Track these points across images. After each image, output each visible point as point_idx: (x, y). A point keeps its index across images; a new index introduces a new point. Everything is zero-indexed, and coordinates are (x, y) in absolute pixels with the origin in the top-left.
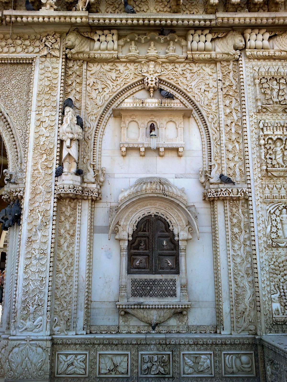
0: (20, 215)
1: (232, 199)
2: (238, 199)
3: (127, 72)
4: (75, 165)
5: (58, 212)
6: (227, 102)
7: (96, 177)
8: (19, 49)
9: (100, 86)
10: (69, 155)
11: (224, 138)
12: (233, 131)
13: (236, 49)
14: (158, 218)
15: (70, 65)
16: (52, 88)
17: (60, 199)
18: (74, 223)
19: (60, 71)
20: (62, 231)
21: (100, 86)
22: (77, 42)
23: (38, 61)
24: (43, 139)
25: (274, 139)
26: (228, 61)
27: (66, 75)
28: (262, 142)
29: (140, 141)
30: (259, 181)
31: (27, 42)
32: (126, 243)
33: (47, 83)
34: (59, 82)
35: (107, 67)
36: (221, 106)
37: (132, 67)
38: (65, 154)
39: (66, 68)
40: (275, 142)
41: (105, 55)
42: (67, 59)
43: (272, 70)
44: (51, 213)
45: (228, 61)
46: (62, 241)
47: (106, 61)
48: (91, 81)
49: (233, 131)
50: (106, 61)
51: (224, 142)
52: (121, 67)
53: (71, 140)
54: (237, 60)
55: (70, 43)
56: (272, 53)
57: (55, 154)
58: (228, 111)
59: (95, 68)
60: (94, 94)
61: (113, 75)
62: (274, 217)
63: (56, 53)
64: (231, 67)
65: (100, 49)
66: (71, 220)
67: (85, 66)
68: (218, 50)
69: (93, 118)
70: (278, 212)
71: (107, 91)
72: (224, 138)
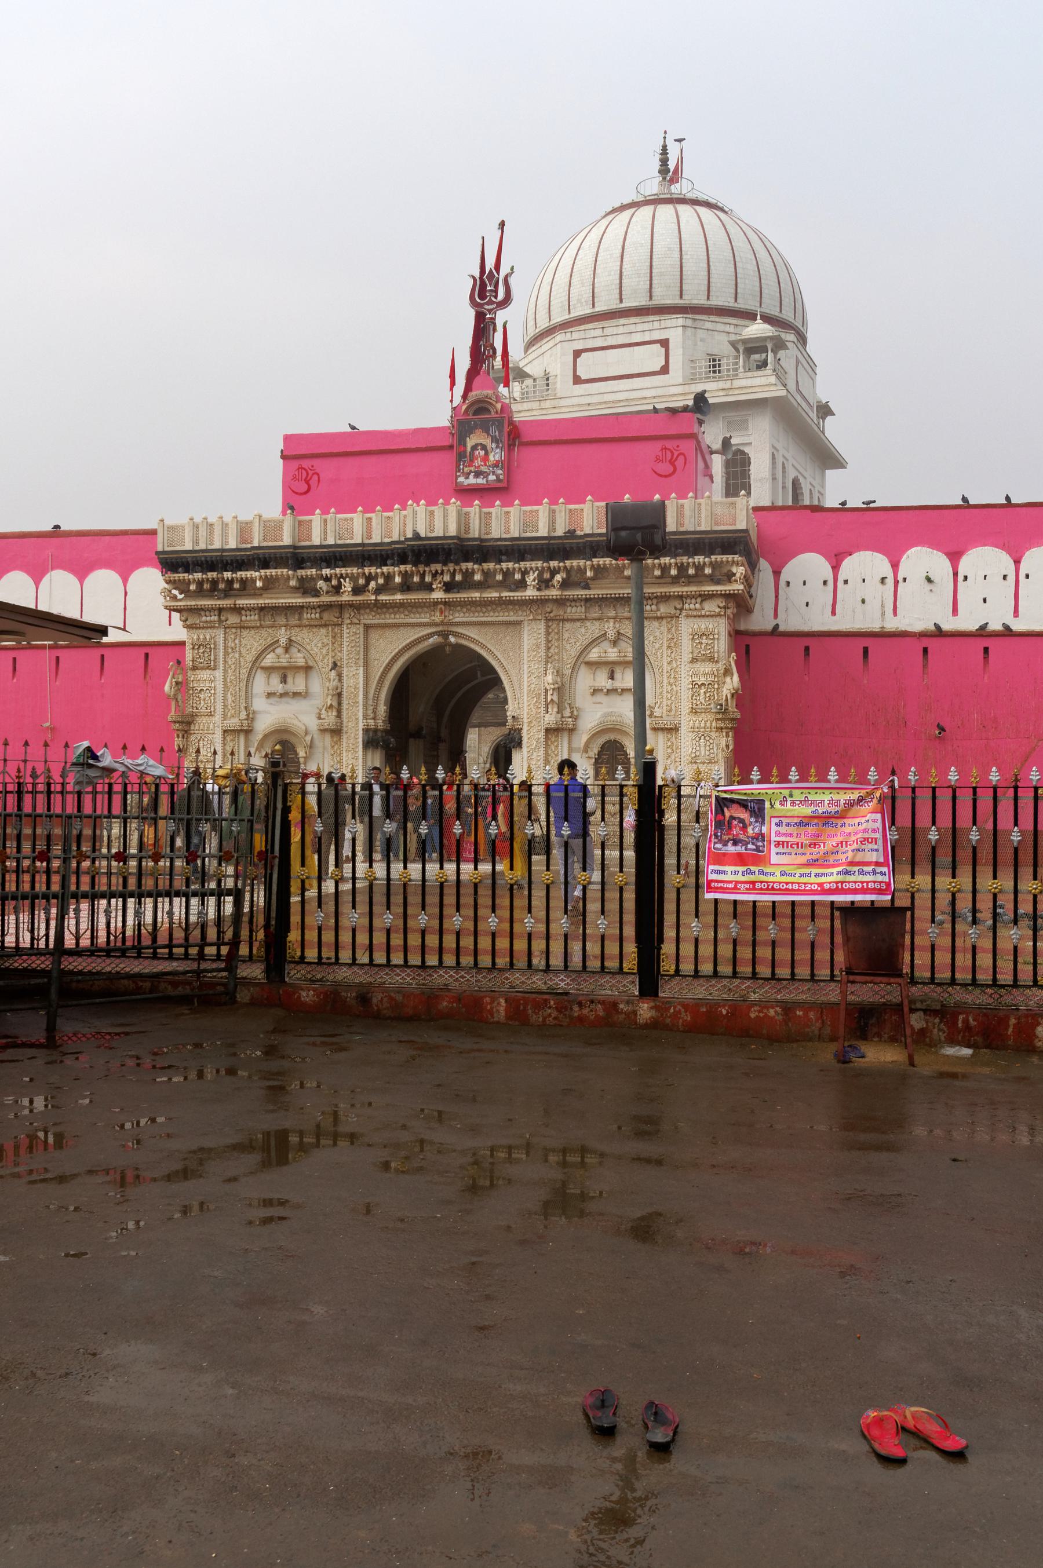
0: (521, 741)
1: (666, 729)
2: (671, 729)
3: (594, 627)
4: (556, 706)
5: (547, 738)
6: (669, 652)
7: (572, 712)
8: (512, 614)
9: (573, 641)
10: (552, 700)
11: (665, 681)
12: (672, 676)
13: (676, 608)
14: (616, 742)
15: (550, 624)
16: (538, 647)
17: (547, 730)
18: (557, 746)
19: (543, 631)
20: (550, 752)
21: (573, 641)
22: (554, 608)
23: (526, 623)
24: (533, 686)
25: (700, 683)
26: (672, 617)
27: (548, 633)
28: (691, 686)
29: (603, 684)
30: (687, 716)
31: (517, 607)
32: (594, 760)
33: (535, 642)
34: (542, 640)
35: (578, 624)
36: (665, 655)
37: (597, 623)
38: (549, 699)
39: (548, 627)
40: (700, 686)
41: (577, 616)
42: (547, 620)
43: (703, 626)
44: (542, 740)
45: (672, 617)
46: (550, 758)
47: (578, 620)
48: (566, 635)
49: (672, 676)
50: (578, 620)
51: (665, 684)
52: (588, 624)
53: (553, 689)
54: (678, 617)
55: (549, 610)
56: (703, 613)
57: (543, 697)
58: (669, 659)
59: (568, 625)
60: (568, 647)
61: (583, 630)
62: (694, 742)
63: (540, 617)
64: (673, 622)
65: (571, 612)
66: (556, 744)
67: (561, 625)
68: (662, 610)
69: (569, 666)
70: (698, 739)
71: (578, 643)
72: (665, 681)
